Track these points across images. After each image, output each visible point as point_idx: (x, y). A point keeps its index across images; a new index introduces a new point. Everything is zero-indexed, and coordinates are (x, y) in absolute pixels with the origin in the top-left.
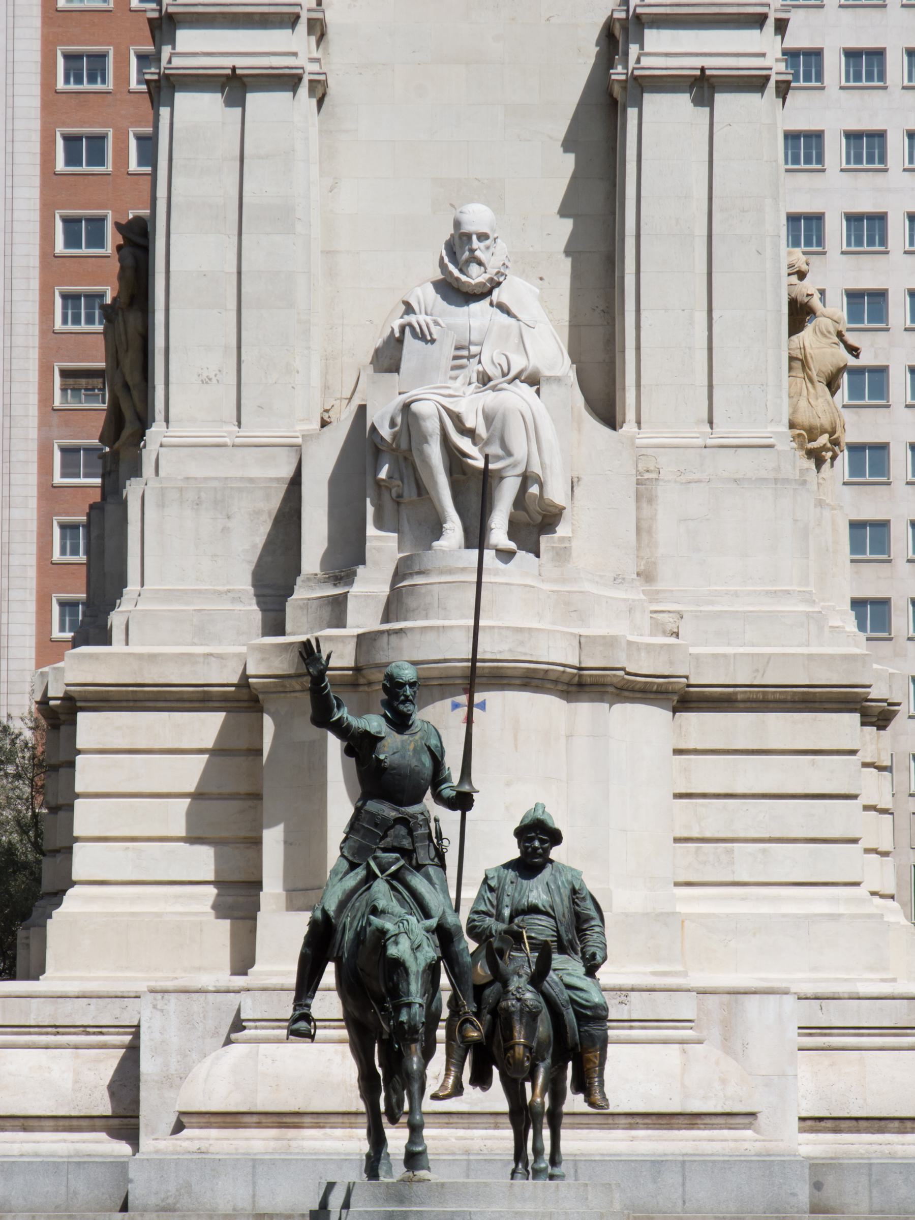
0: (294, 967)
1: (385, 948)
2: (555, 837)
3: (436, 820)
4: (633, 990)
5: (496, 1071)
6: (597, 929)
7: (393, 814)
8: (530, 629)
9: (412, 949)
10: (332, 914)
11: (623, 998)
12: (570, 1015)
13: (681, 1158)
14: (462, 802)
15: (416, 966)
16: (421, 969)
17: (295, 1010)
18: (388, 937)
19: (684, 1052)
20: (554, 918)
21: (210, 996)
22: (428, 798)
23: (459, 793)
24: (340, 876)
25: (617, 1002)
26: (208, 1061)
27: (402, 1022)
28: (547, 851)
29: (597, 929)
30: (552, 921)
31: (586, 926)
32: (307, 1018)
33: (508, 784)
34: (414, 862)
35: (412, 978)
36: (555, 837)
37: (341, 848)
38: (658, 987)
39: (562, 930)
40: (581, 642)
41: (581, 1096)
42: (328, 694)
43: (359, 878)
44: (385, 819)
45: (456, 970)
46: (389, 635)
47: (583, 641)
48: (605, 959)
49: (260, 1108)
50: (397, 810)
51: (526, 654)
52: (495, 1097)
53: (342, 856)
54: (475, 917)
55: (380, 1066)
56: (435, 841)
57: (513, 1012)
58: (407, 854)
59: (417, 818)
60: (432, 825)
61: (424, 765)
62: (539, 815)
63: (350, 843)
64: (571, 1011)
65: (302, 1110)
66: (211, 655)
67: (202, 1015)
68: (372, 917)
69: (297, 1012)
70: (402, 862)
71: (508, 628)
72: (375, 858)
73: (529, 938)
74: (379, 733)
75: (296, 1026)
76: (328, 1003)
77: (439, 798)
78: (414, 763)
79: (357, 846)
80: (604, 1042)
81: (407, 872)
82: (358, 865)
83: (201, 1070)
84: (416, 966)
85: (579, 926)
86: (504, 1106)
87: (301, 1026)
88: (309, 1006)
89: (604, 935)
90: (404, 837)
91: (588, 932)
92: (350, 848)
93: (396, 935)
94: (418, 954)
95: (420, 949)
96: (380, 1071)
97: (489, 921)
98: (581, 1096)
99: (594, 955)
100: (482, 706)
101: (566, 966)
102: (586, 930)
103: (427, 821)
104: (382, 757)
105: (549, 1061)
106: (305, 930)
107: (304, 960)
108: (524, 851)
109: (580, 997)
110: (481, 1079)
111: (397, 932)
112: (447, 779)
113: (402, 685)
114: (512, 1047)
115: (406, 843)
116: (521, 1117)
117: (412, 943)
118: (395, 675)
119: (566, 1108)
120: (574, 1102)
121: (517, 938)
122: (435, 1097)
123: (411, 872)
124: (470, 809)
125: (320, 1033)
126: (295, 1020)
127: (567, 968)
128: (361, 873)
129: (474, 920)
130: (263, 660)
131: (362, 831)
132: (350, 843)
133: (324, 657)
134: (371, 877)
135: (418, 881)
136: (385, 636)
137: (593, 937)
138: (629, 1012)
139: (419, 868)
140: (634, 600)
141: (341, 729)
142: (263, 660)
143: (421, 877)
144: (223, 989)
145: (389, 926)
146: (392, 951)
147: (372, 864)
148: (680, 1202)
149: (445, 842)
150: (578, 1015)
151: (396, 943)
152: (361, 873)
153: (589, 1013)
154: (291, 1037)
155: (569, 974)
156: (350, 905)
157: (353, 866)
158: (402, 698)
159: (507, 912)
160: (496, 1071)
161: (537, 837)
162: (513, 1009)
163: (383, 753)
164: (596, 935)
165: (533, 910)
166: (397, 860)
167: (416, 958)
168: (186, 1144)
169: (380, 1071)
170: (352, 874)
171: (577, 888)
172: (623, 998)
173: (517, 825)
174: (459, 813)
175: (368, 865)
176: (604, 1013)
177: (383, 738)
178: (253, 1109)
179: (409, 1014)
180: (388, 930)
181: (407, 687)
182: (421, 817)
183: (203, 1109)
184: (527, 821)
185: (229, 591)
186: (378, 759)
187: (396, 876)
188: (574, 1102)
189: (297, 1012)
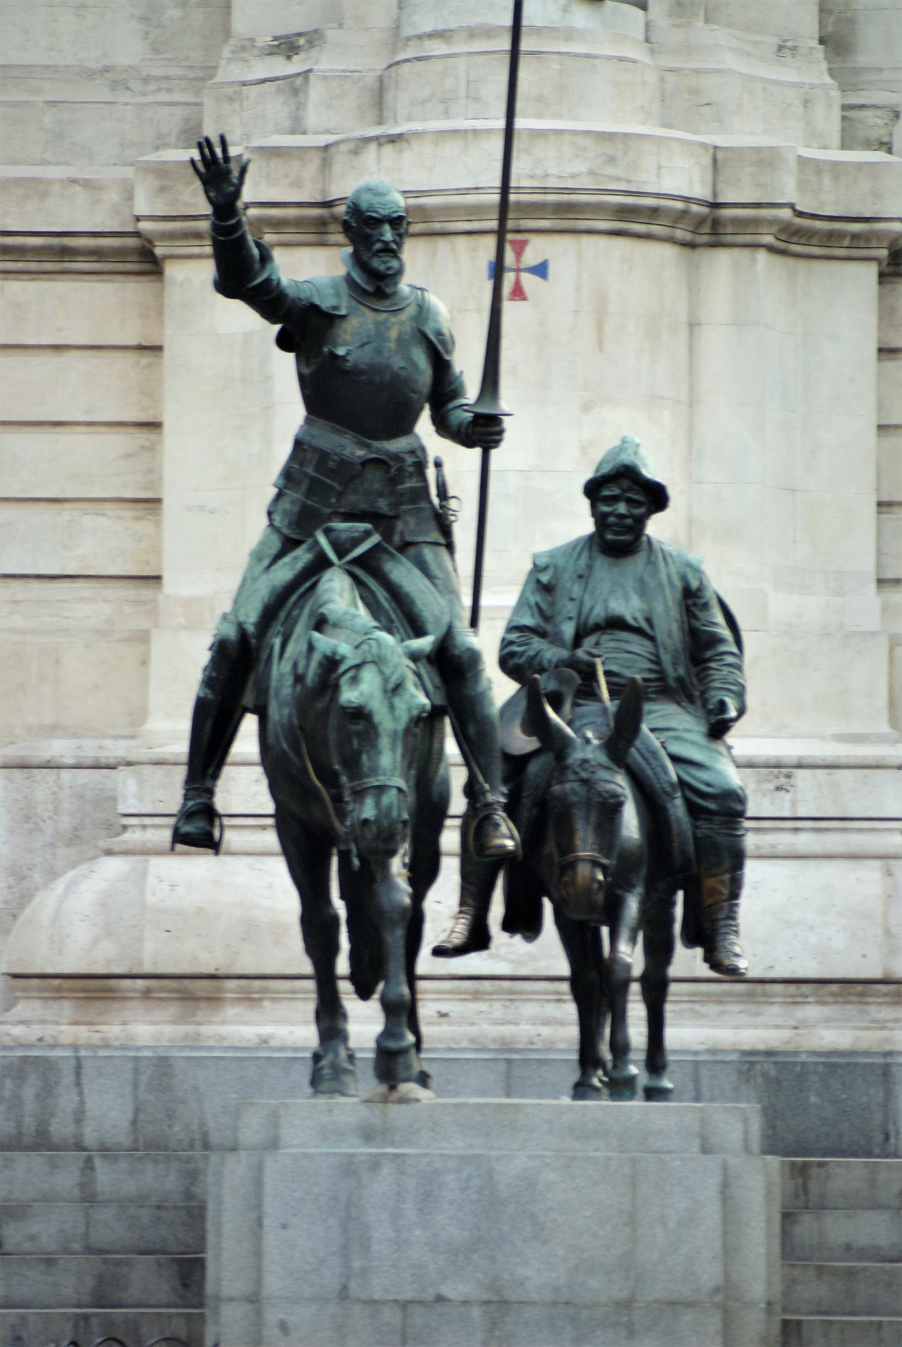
0: (185, 725)
1: (336, 688)
2: (656, 497)
3: (438, 465)
4: (800, 766)
5: (548, 907)
6: (730, 659)
7: (360, 452)
8: (626, 135)
9: (385, 691)
10: (250, 629)
11: (783, 781)
12: (677, 808)
13: (881, 1060)
14: (483, 432)
15: (390, 721)
16: (401, 726)
17: (186, 798)
18: (342, 668)
19: (889, 873)
20: (652, 639)
21: (66, 774)
22: (424, 427)
23: (478, 416)
24: (266, 562)
25: (771, 786)
26: (60, 886)
27: (366, 822)
28: (640, 523)
29: (730, 659)
30: (648, 643)
31: (709, 654)
32: (209, 813)
33: (587, 407)
34: (397, 538)
35: (384, 742)
36: (656, 497)
37: (270, 514)
38: (843, 761)
39: (666, 659)
40: (718, 161)
41: (699, 952)
42: (243, 238)
43: (300, 565)
44: (344, 463)
45: (472, 729)
46: (380, 145)
47: (720, 156)
48: (741, 712)
49: (148, 969)
50: (368, 446)
51: (618, 179)
52: (548, 952)
53: (271, 525)
54: (513, 636)
55: (343, 897)
56: (436, 501)
57: (572, 805)
58: (381, 521)
59: (402, 460)
60: (431, 473)
61: (414, 365)
62: (626, 458)
63: (285, 504)
64: (679, 802)
65: (222, 972)
66: (74, 181)
67: (50, 807)
68: (316, 635)
69: (190, 803)
70: (376, 539)
71: (587, 133)
72: (328, 532)
73: (607, 673)
74: (336, 308)
75: (186, 828)
76: (244, 786)
77: (442, 426)
78: (397, 362)
79: (296, 509)
80: (737, 858)
81: (385, 557)
82: (297, 543)
83: (46, 902)
84: (390, 721)
85: (697, 657)
86: (563, 967)
87: (198, 829)
88: (210, 793)
89: (739, 668)
90: (380, 494)
91: (713, 665)
92: (285, 513)
93: (358, 667)
94: (397, 701)
95: (400, 691)
96: (340, 907)
97: (537, 644)
98: (699, 952)
99: (722, 706)
100: (541, 270)
101: (673, 724)
102: (710, 660)
103: (420, 466)
104: (341, 351)
105: (639, 890)
106: (204, 657)
107: (201, 709)
108: (600, 520)
109: (695, 778)
110: (523, 922)
111: (358, 661)
112: (457, 393)
113: (378, 222)
114: (572, 865)
115: (383, 505)
116: (594, 988)
117: (386, 680)
118: (364, 206)
119: (674, 970)
120: (687, 960)
121: (589, 674)
122: (438, 952)
123: (392, 555)
124: (496, 443)
125: (231, 838)
126: (187, 815)
127: (671, 729)
128: (301, 557)
129: (511, 643)
130: (162, 190)
131: (305, 485)
132: (285, 504)
133: (235, 173)
134: (320, 564)
135: (403, 573)
136: (373, 147)
137: (719, 673)
138: (794, 803)
139: (404, 547)
140: (812, 87)
141: (269, 300)
142: (162, 190)
143: (409, 564)
144: (89, 762)
145: (344, 649)
146: (349, 695)
147: (323, 540)
148: (880, 1138)
149: (453, 504)
150: (693, 810)
151: (355, 680)
152: (301, 557)
153: (712, 806)
154: (179, 847)
155: (677, 739)
156: (282, 615)
157: (289, 545)
158: (378, 246)
159: (568, 630)
160: (548, 907)
161: (624, 498)
162: (574, 799)
163: (345, 344)
164: (726, 670)
165: (616, 624)
166: (367, 534)
167: (392, 707)
168: (18, 1031)
169: (340, 907)
170: (286, 559)
171: (694, 584)
172: (783, 781)
173: (589, 475)
174: (477, 452)
175: (316, 543)
176: (739, 807)
177: (343, 317)
178: (136, 971)
179: (378, 804)
180: (343, 658)
181: (387, 228)
182: (410, 460)
183: (49, 970)
184: (605, 470)
185: (106, 70)
186: (334, 356)
187: (362, 561)
188: (687, 960)
189: (190, 803)
